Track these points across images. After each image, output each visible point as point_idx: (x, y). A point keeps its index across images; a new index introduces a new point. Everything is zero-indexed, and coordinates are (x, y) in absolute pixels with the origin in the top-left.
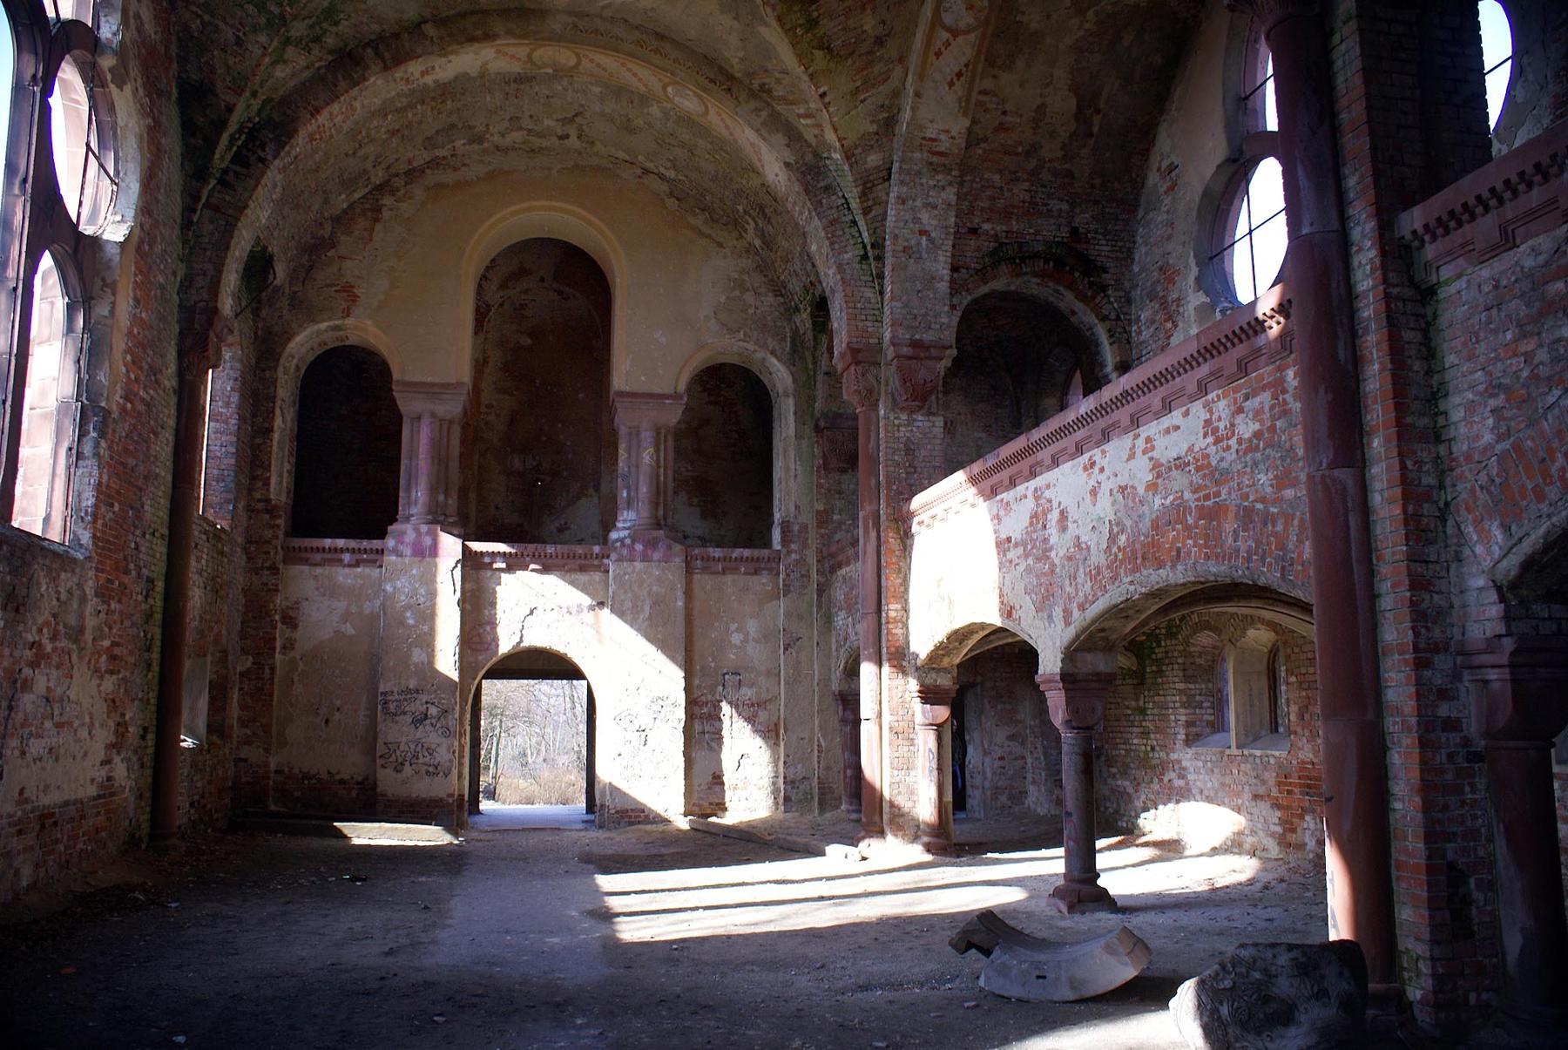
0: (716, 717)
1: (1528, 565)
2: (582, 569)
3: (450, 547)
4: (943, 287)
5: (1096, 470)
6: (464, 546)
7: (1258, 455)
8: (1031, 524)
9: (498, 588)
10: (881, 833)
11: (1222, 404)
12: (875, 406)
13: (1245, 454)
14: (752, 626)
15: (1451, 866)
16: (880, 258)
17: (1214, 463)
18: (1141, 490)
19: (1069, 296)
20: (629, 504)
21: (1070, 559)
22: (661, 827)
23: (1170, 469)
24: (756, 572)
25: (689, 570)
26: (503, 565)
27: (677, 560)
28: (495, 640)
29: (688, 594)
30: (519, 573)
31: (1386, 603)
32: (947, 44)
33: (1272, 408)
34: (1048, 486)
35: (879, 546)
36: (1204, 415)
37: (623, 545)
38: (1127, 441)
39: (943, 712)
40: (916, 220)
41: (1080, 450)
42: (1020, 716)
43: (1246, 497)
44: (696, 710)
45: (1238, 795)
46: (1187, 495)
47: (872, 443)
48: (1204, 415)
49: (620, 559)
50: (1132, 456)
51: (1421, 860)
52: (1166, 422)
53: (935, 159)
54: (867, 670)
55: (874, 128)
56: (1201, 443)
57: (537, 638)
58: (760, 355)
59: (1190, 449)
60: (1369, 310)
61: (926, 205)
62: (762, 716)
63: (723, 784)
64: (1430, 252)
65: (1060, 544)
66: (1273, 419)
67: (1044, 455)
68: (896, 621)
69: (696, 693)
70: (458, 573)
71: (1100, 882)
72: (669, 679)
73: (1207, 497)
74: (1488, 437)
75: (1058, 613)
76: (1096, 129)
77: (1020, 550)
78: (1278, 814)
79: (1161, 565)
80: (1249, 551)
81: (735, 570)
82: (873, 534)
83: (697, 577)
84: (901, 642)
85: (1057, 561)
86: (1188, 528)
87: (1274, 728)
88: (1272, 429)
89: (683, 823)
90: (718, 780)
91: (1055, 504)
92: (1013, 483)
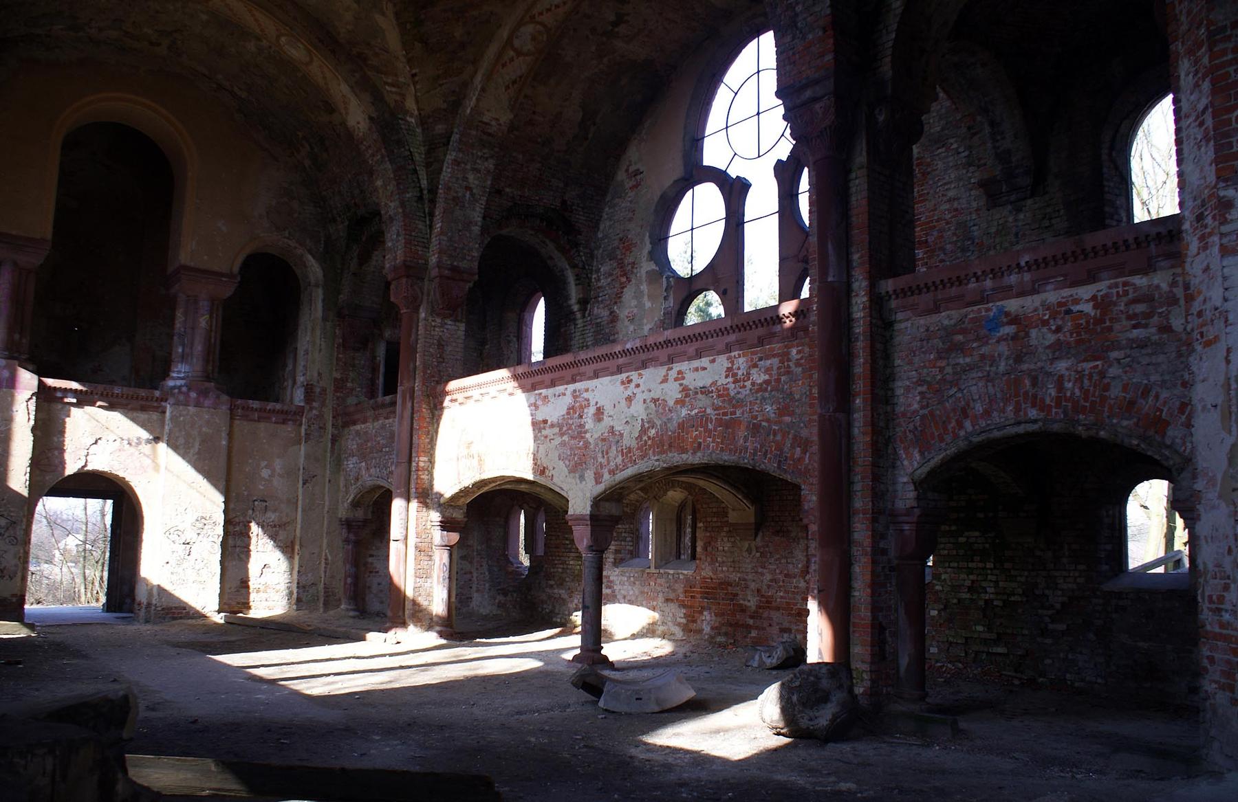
0: (246, 535)
1: (932, 473)
2: (143, 409)
3: (27, 381)
4: (476, 229)
5: (632, 385)
6: (40, 382)
7: (767, 395)
8: (568, 413)
9: (67, 420)
10: (404, 624)
11: (741, 360)
12: (416, 310)
13: (757, 392)
14: (278, 464)
15: (880, 624)
16: (433, 201)
17: (732, 394)
18: (671, 403)
19: (551, 246)
20: (184, 358)
21: (604, 440)
22: (200, 622)
23: (696, 393)
24: (284, 422)
25: (232, 419)
26: (74, 401)
27: (224, 407)
28: (62, 463)
29: (230, 435)
30: (88, 409)
31: (858, 487)
32: (512, 60)
33: (779, 368)
34: (587, 390)
35: (412, 413)
36: (727, 364)
37: (180, 392)
38: (662, 371)
39: (455, 537)
40: (465, 179)
41: (619, 370)
42: (470, 542)
43: (756, 417)
44: (231, 528)
45: (654, 599)
46: (709, 411)
47: (413, 337)
48: (727, 364)
49: (177, 403)
50: (665, 380)
51: (868, 621)
52: (696, 363)
53: (485, 137)
54: (397, 505)
55: (444, 106)
56: (722, 381)
57: (100, 462)
58: (300, 251)
59: (714, 383)
60: (859, 329)
61: (474, 169)
62: (282, 535)
63: (248, 587)
64: (893, 304)
65: (594, 431)
66: (779, 374)
67: (588, 369)
68: (424, 470)
69: (232, 515)
70: (33, 402)
71: (603, 652)
72: (212, 502)
73: (725, 414)
74: (916, 406)
75: (590, 475)
76: (590, 136)
77: (556, 430)
78: (684, 611)
79: (684, 451)
80: (755, 450)
81: (268, 419)
82: (409, 405)
83: (237, 422)
84: (426, 486)
85: (591, 440)
86: (706, 430)
87: (678, 557)
88: (778, 380)
89: (219, 619)
90: (244, 584)
91: (592, 403)
92: (553, 384)
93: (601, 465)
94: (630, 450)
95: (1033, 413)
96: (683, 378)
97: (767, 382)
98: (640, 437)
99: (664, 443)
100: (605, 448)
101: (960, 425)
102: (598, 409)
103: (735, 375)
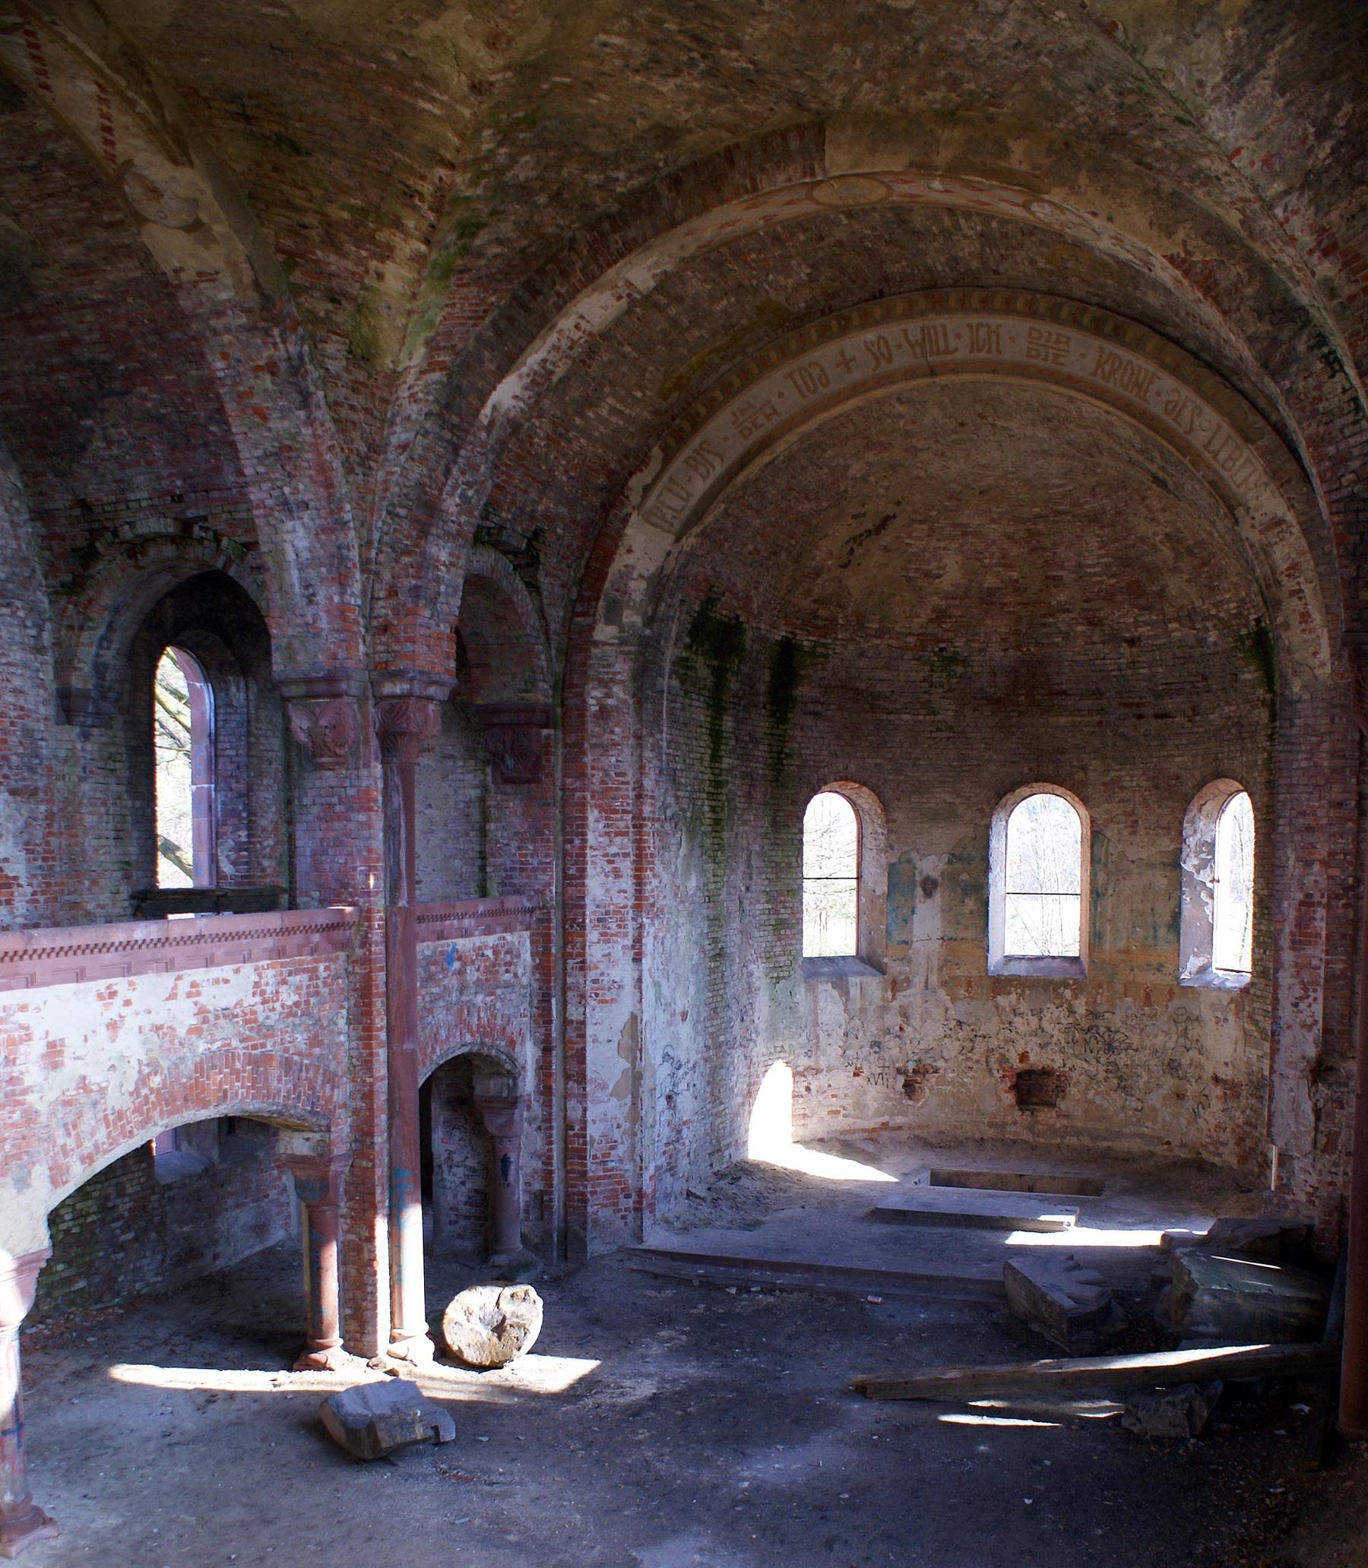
5: (118, 1001)
11: (270, 973)
18: (182, 1032)
23: (217, 1017)
34: (23, 1008)
36: (255, 978)
38: (167, 980)
46: (235, 1043)
48: (255, 978)
50: (173, 996)
52: (216, 972)
56: (250, 1000)
59: (239, 1003)
66: (309, 995)
73: (254, 1047)
79: (205, 1104)
88: (307, 1002)
91: (38, 1032)
93: (65, 1151)
94: (120, 1115)
95: (468, 1038)
96: (199, 994)
97: (297, 1004)
98: (137, 1091)
99: (167, 1099)
100: (71, 1117)
101: (434, 1051)
102: (51, 1045)
103: (263, 993)
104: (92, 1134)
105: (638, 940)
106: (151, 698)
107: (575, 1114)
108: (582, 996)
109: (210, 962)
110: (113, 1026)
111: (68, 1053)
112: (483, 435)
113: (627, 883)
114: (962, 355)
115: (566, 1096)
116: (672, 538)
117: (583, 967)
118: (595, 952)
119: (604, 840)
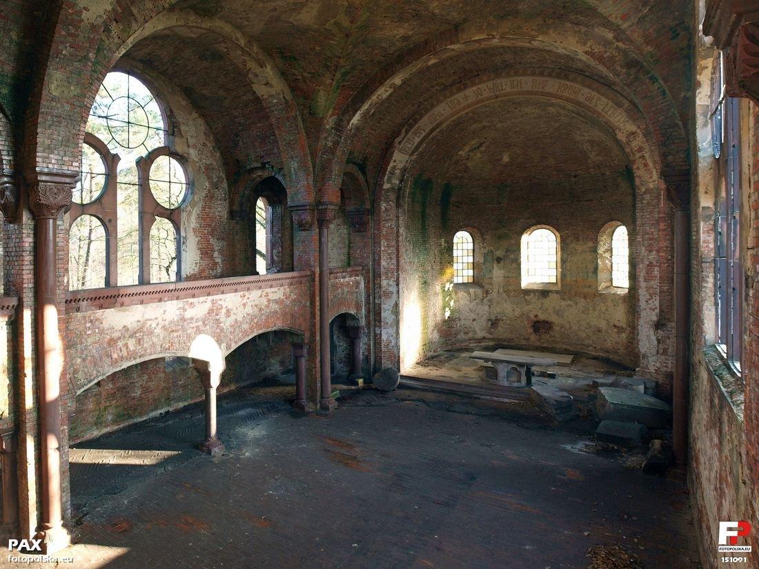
5: (246, 297)
8: (208, 313)
52: (273, 290)
91: (224, 307)
102: (228, 310)
104: (238, 335)
105: (398, 279)
106: (255, 212)
107: (378, 331)
108: (380, 296)
109: (271, 287)
110: (244, 305)
111: (232, 312)
112: (349, 132)
113: (394, 261)
114: (508, 90)
115: (375, 326)
116: (408, 156)
117: (380, 287)
118: (384, 283)
119: (387, 249)
